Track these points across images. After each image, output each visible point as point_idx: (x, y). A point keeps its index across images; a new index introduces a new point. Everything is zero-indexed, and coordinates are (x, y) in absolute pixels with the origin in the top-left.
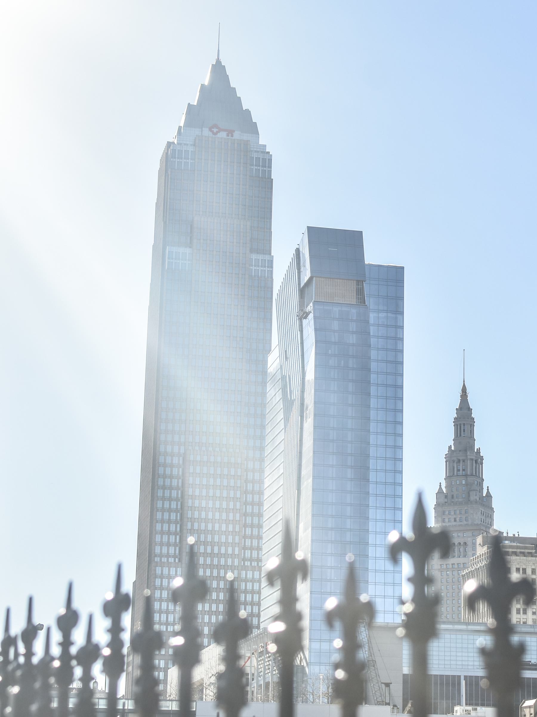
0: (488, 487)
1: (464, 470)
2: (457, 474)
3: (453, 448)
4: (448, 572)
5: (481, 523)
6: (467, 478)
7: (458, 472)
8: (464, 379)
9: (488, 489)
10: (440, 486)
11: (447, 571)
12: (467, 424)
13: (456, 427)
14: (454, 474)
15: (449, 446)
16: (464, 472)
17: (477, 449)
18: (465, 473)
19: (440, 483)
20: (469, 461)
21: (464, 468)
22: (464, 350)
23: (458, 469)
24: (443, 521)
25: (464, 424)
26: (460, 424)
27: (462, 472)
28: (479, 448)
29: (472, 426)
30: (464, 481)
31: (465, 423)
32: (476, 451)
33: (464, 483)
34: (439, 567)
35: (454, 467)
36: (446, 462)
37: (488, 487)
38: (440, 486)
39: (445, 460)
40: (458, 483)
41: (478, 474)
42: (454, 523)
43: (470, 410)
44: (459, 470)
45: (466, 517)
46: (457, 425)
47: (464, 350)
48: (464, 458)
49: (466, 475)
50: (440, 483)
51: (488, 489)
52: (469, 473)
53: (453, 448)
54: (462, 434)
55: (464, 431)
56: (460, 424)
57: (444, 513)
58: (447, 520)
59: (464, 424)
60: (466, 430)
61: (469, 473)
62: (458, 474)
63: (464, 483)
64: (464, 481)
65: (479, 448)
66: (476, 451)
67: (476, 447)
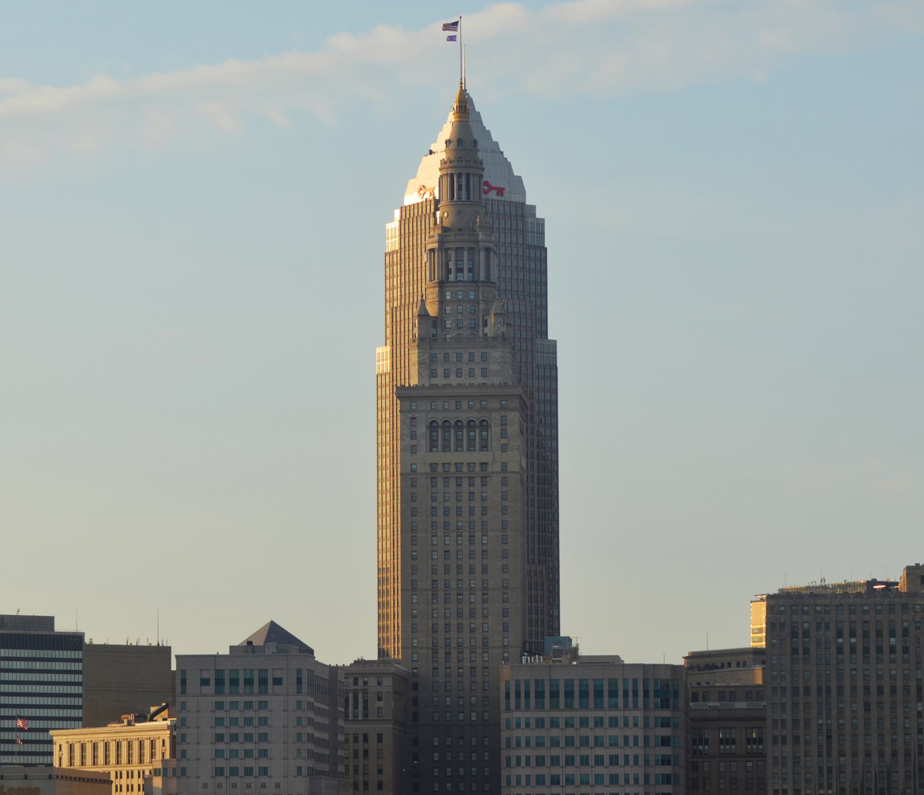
1: (471, 270)
6: (478, 287)
7: (459, 274)
12: (474, 174)
16: (471, 275)
20: (482, 254)
21: (471, 267)
22: (461, 17)
24: (433, 374)
25: (468, 175)
27: (456, 275)
30: (472, 293)
31: (470, 171)
33: (472, 297)
34: (428, 470)
40: (460, 297)
42: (460, 381)
44: (459, 270)
46: (452, 175)
47: (461, 17)
48: (472, 245)
49: (475, 282)
57: (433, 359)
58: (440, 372)
59: (468, 175)
61: (482, 277)
62: (459, 279)
63: (472, 297)
64: (472, 293)
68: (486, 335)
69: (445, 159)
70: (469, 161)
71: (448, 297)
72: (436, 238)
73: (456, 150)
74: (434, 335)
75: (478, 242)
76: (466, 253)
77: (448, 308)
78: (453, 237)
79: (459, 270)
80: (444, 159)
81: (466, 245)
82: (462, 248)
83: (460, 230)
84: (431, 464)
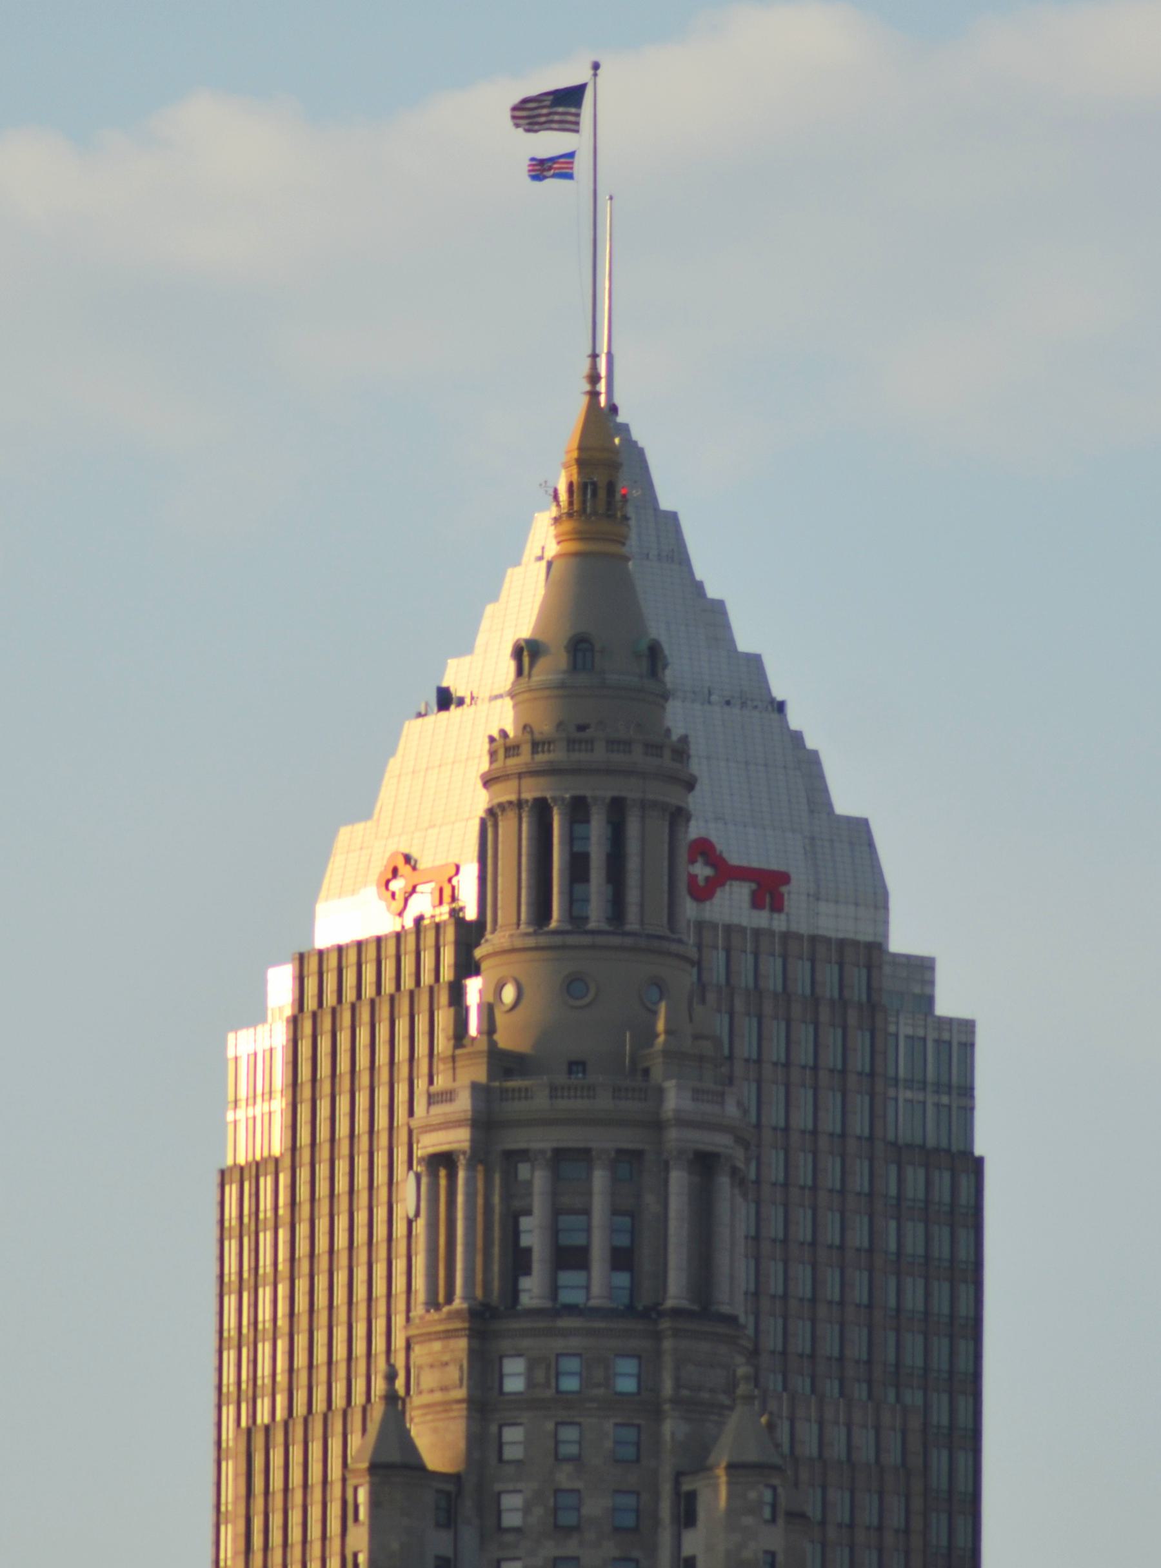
1: (621, 1259)
2: (554, 1289)
6: (657, 1336)
7: (567, 1278)
12: (645, 806)
16: (622, 1279)
20: (678, 1180)
21: (623, 1241)
22: (596, 66)
23: (566, 1240)
25: (617, 809)
30: (628, 1366)
31: (630, 790)
33: (627, 1385)
40: (570, 1384)
46: (542, 809)
47: (596, 66)
48: (627, 1139)
59: (617, 809)
61: (676, 1291)
62: (566, 1297)
63: (627, 1385)
69: (511, 734)
70: (624, 745)
71: (514, 1384)
72: (463, 1103)
73: (564, 690)
75: (657, 1125)
77: (512, 1434)
78: (541, 1102)
80: (504, 734)
81: (603, 1141)
82: (584, 1155)
83: (576, 1066)
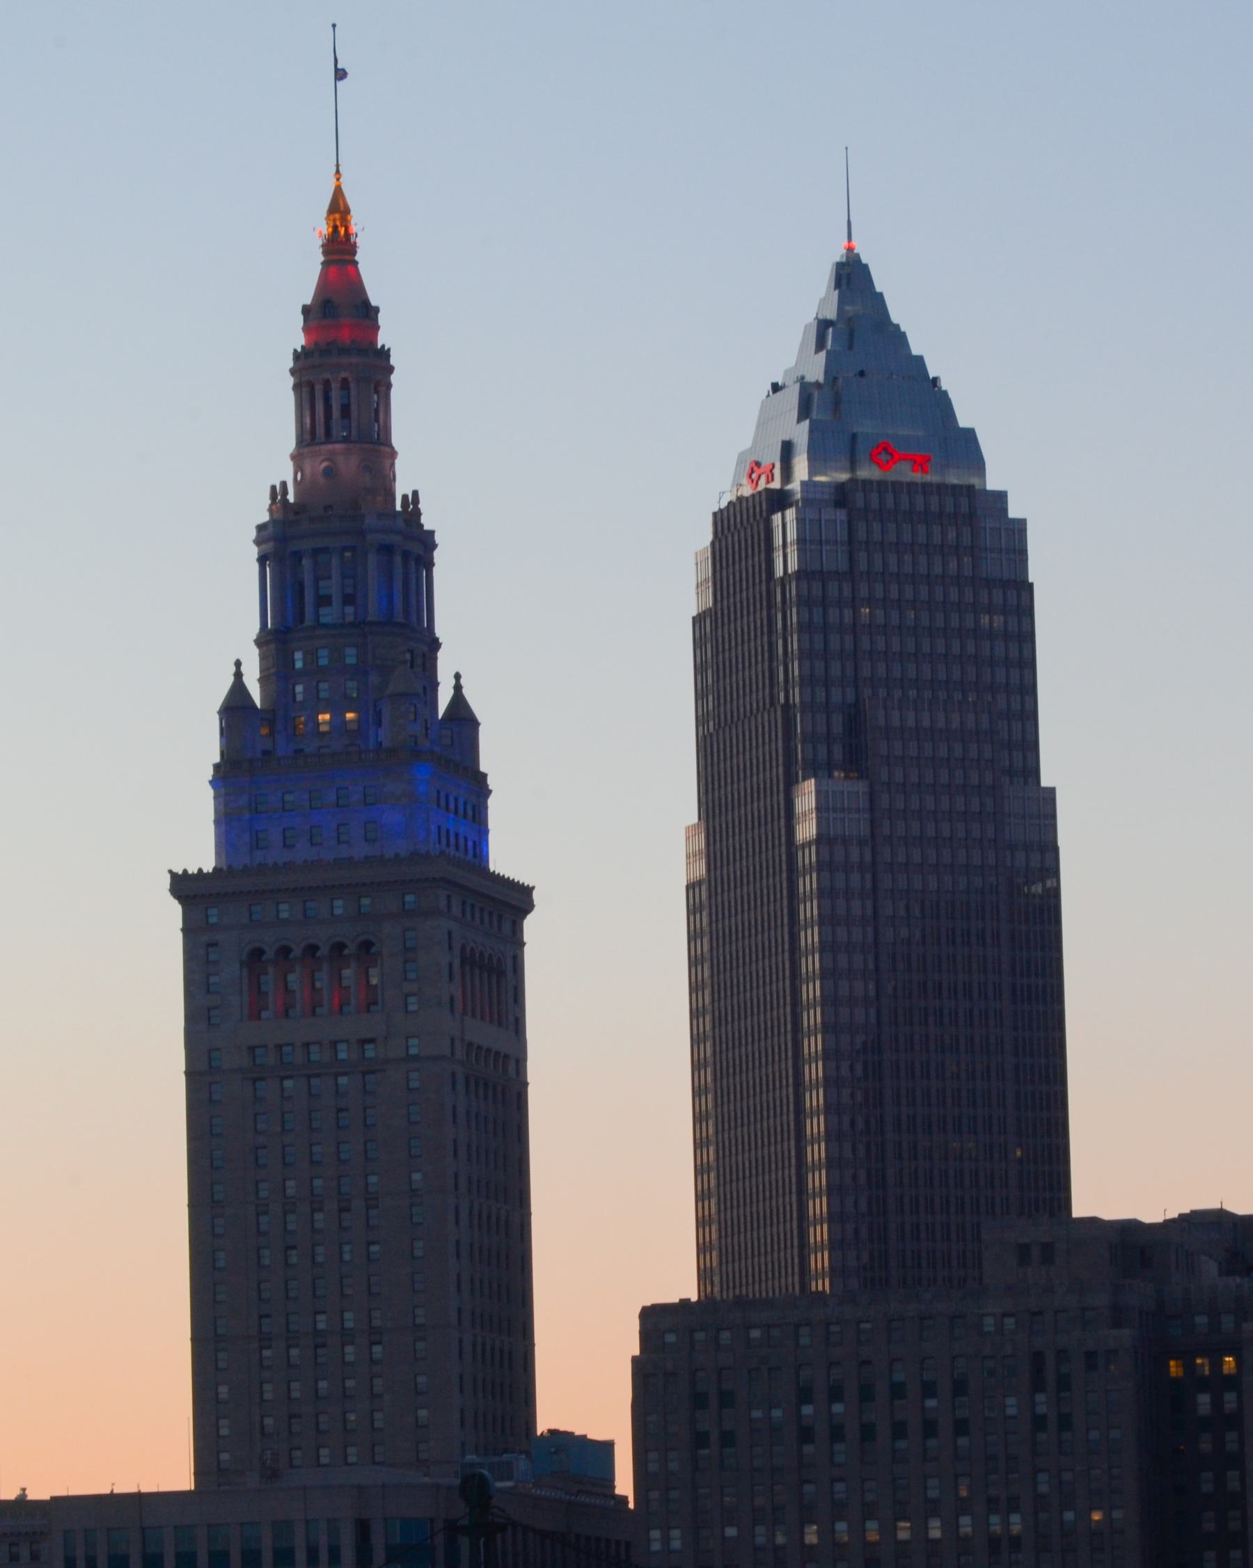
0: (458, 677)
1: (348, 599)
3: (291, 498)
4: (288, 1084)
5: (442, 853)
7: (323, 611)
8: (338, 165)
9: (458, 688)
10: (238, 675)
11: (283, 1078)
13: (305, 395)
14: (301, 617)
15: (273, 488)
16: (350, 610)
17: (405, 497)
18: (355, 614)
19: (238, 664)
20: (372, 559)
21: (349, 590)
22: (334, 26)
23: (321, 593)
25: (345, 384)
26: (327, 385)
28: (415, 493)
29: (382, 388)
32: (398, 508)
33: (351, 660)
35: (301, 585)
36: (262, 560)
37: (458, 677)
38: (238, 675)
39: (254, 552)
40: (324, 662)
41: (414, 618)
43: (368, 314)
45: (338, 826)
47: (334, 26)
50: (238, 664)
51: (458, 688)
52: (373, 612)
53: (291, 498)
54: (334, 432)
55: (346, 411)
56: (327, 385)
60: (353, 408)
61: (373, 612)
63: (351, 660)
65: (415, 493)
66: (398, 508)
67: (402, 488)
68: (381, 743)
74: (266, 753)
76: (306, 563)
79: (323, 600)
82: (325, 550)
84: (252, 1049)
